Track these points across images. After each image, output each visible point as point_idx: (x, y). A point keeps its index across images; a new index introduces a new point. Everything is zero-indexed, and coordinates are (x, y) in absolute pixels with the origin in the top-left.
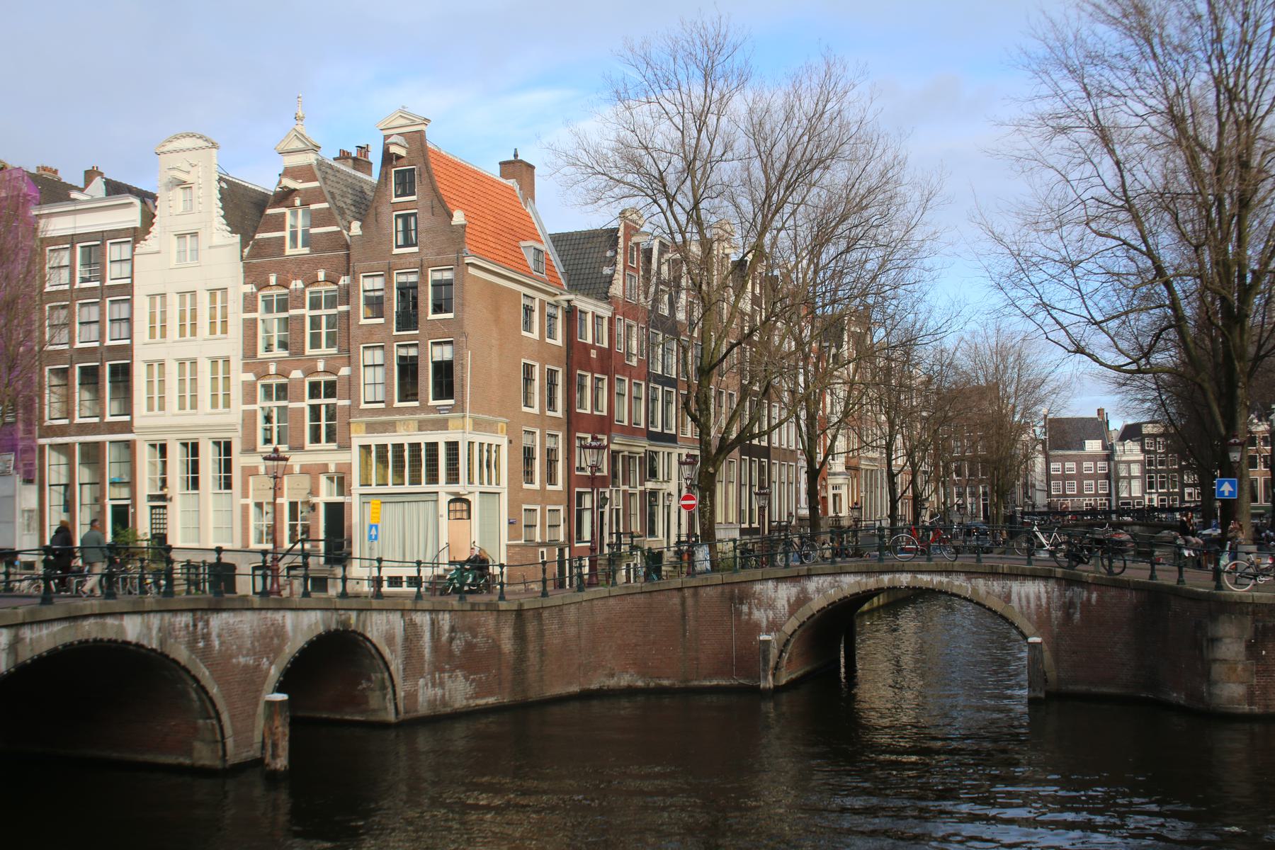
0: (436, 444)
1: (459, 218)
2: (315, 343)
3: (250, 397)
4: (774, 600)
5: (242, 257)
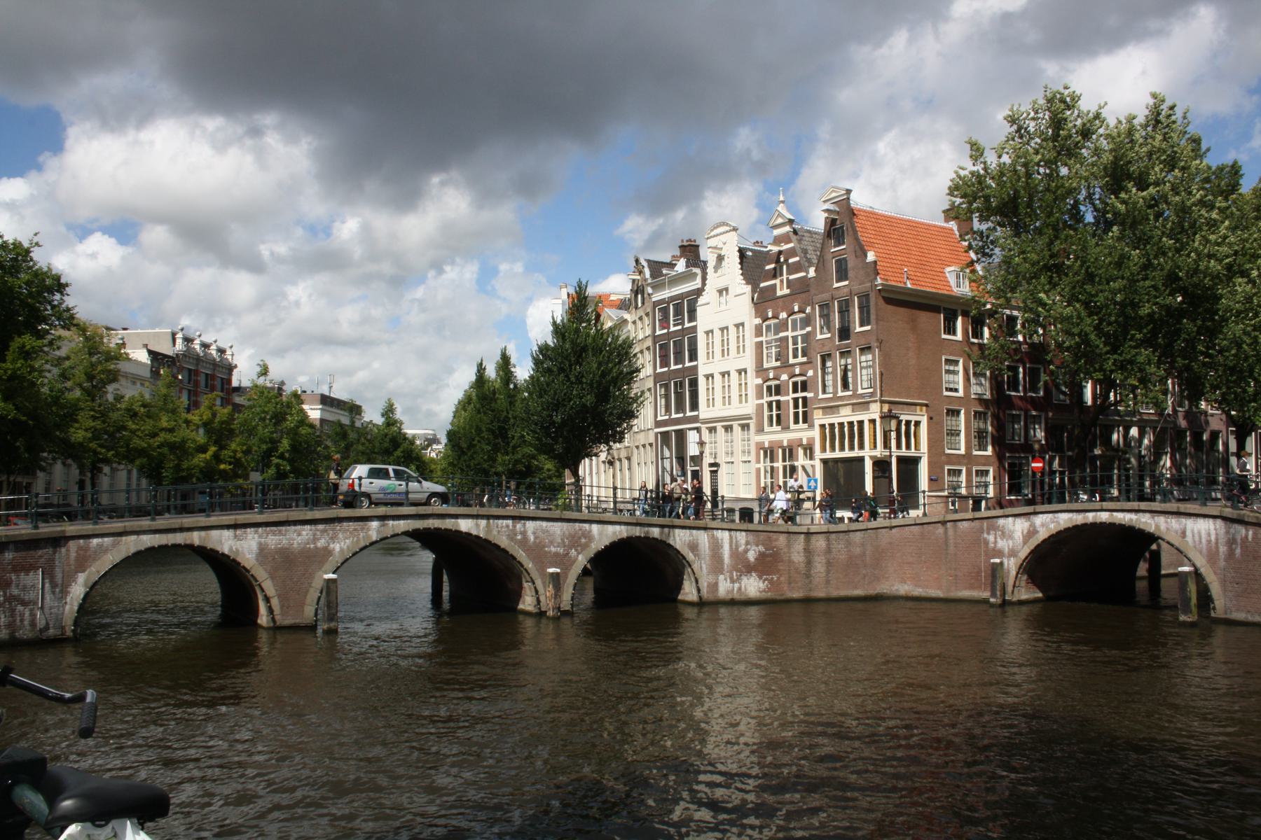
1: (871, 257)
2: (795, 356)
3: (760, 396)
5: (753, 299)
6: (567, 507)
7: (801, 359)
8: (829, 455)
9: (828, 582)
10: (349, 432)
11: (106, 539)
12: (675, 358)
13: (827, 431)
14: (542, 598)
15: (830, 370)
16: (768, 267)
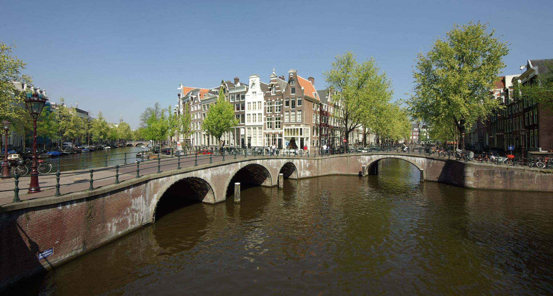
0: (298, 129)
1: (303, 88)
2: (277, 111)
3: (265, 120)
4: (365, 159)
7: (278, 112)
8: (286, 137)
9: (321, 171)
11: (164, 178)
16: (269, 88)
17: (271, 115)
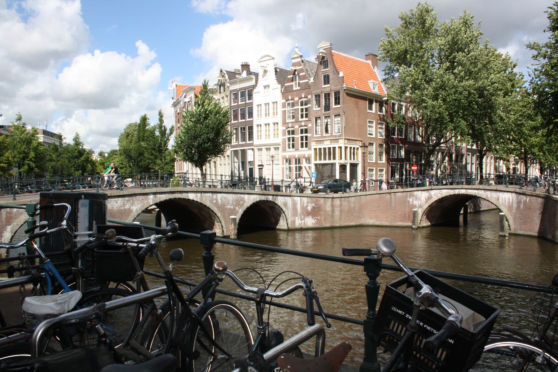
1: (341, 74)
2: (302, 117)
3: (284, 135)
6: (178, 185)
8: (318, 162)
9: (340, 219)
10: (59, 148)
12: (241, 116)
13: (318, 151)
14: (225, 230)
15: (319, 124)
16: (289, 77)
17: (294, 124)
